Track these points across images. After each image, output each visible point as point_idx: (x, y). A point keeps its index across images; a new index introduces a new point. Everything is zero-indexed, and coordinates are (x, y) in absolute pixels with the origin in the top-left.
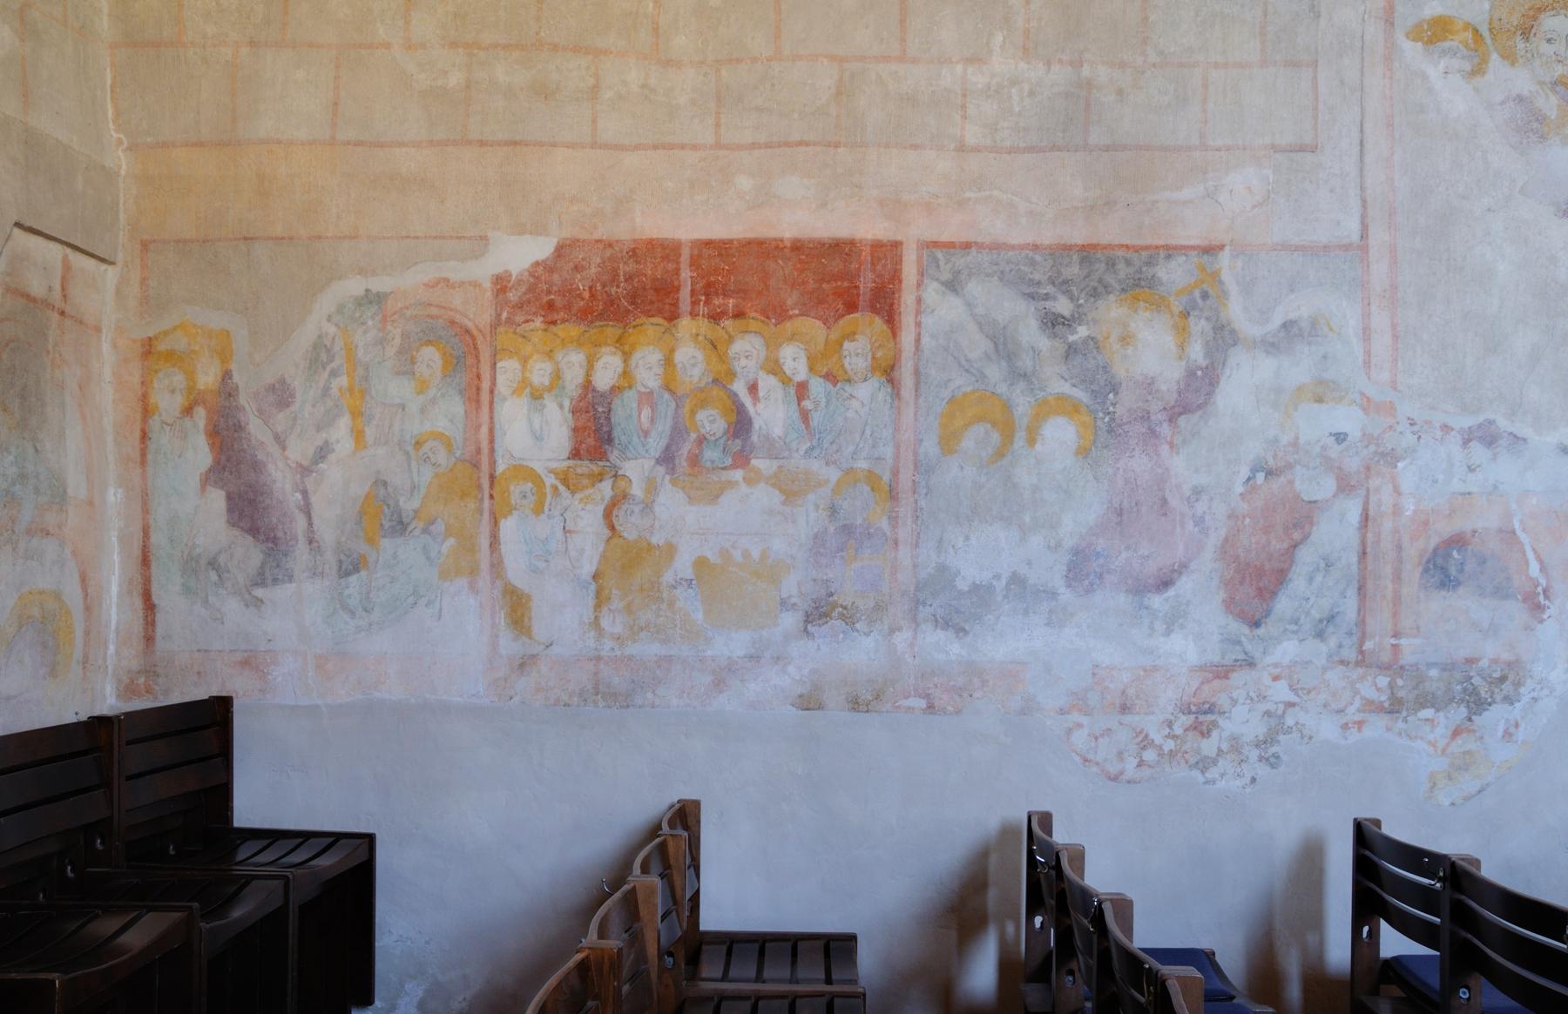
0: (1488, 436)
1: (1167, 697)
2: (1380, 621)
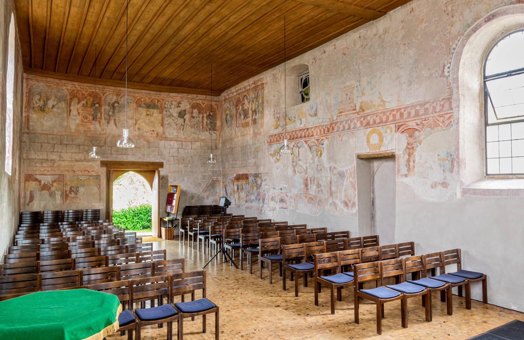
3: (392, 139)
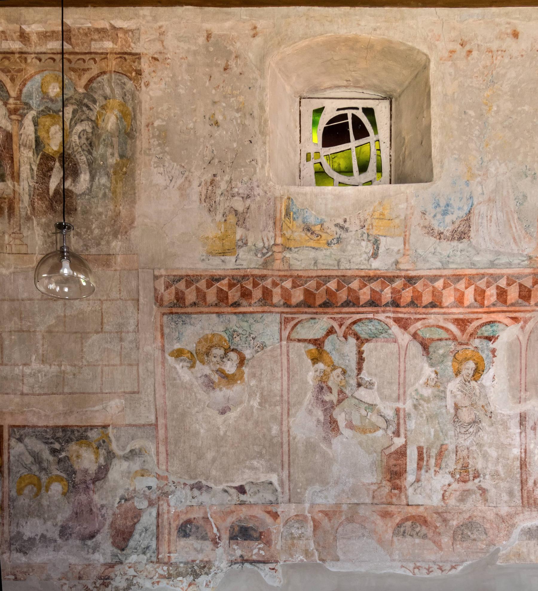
0: (199, 487)
1: (94, 574)
2: (164, 548)
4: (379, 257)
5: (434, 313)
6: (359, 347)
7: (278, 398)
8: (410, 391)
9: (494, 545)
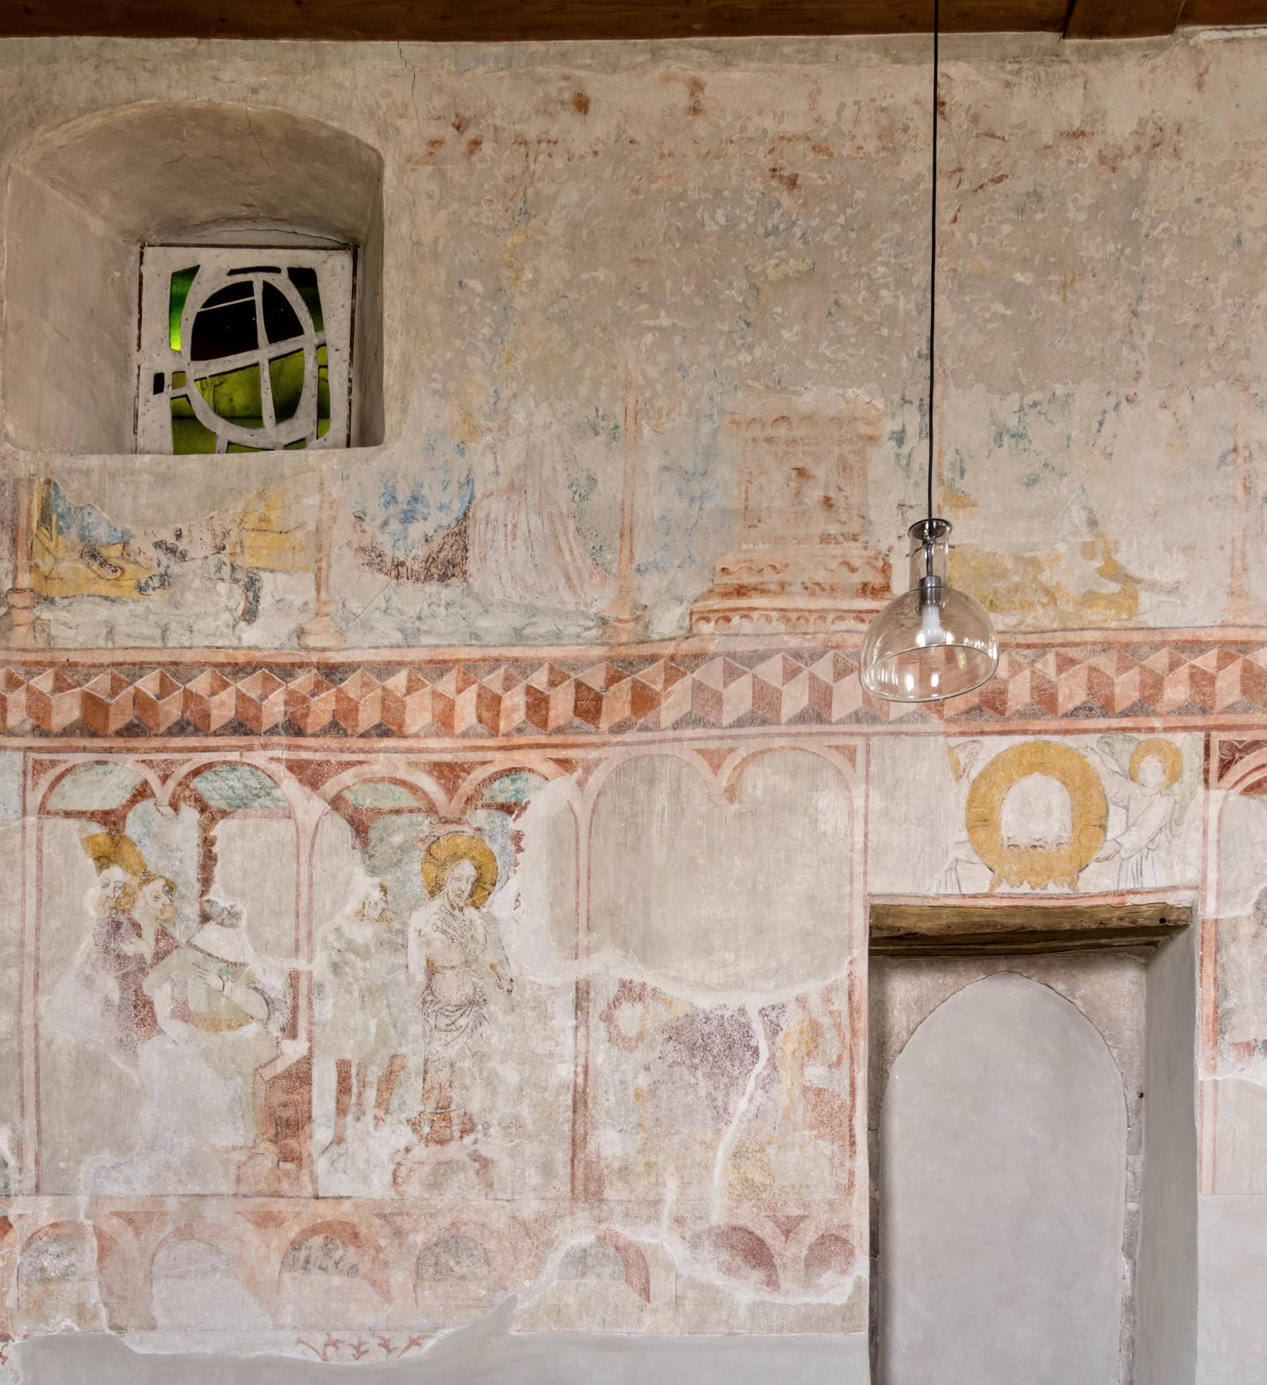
3: (1173, 823)
4: (260, 621)
5: (386, 750)
6: (205, 829)
7: (13, 950)
8: (323, 931)
9: (505, 1289)
